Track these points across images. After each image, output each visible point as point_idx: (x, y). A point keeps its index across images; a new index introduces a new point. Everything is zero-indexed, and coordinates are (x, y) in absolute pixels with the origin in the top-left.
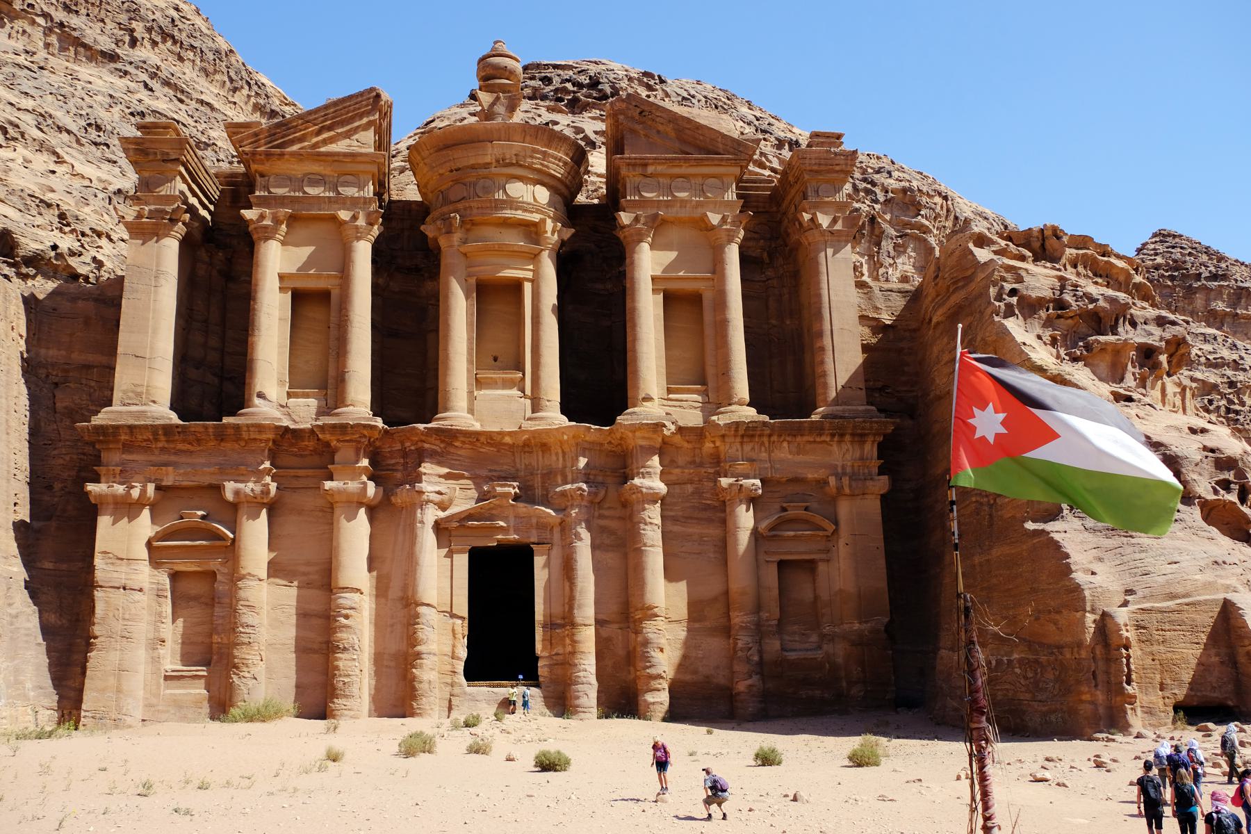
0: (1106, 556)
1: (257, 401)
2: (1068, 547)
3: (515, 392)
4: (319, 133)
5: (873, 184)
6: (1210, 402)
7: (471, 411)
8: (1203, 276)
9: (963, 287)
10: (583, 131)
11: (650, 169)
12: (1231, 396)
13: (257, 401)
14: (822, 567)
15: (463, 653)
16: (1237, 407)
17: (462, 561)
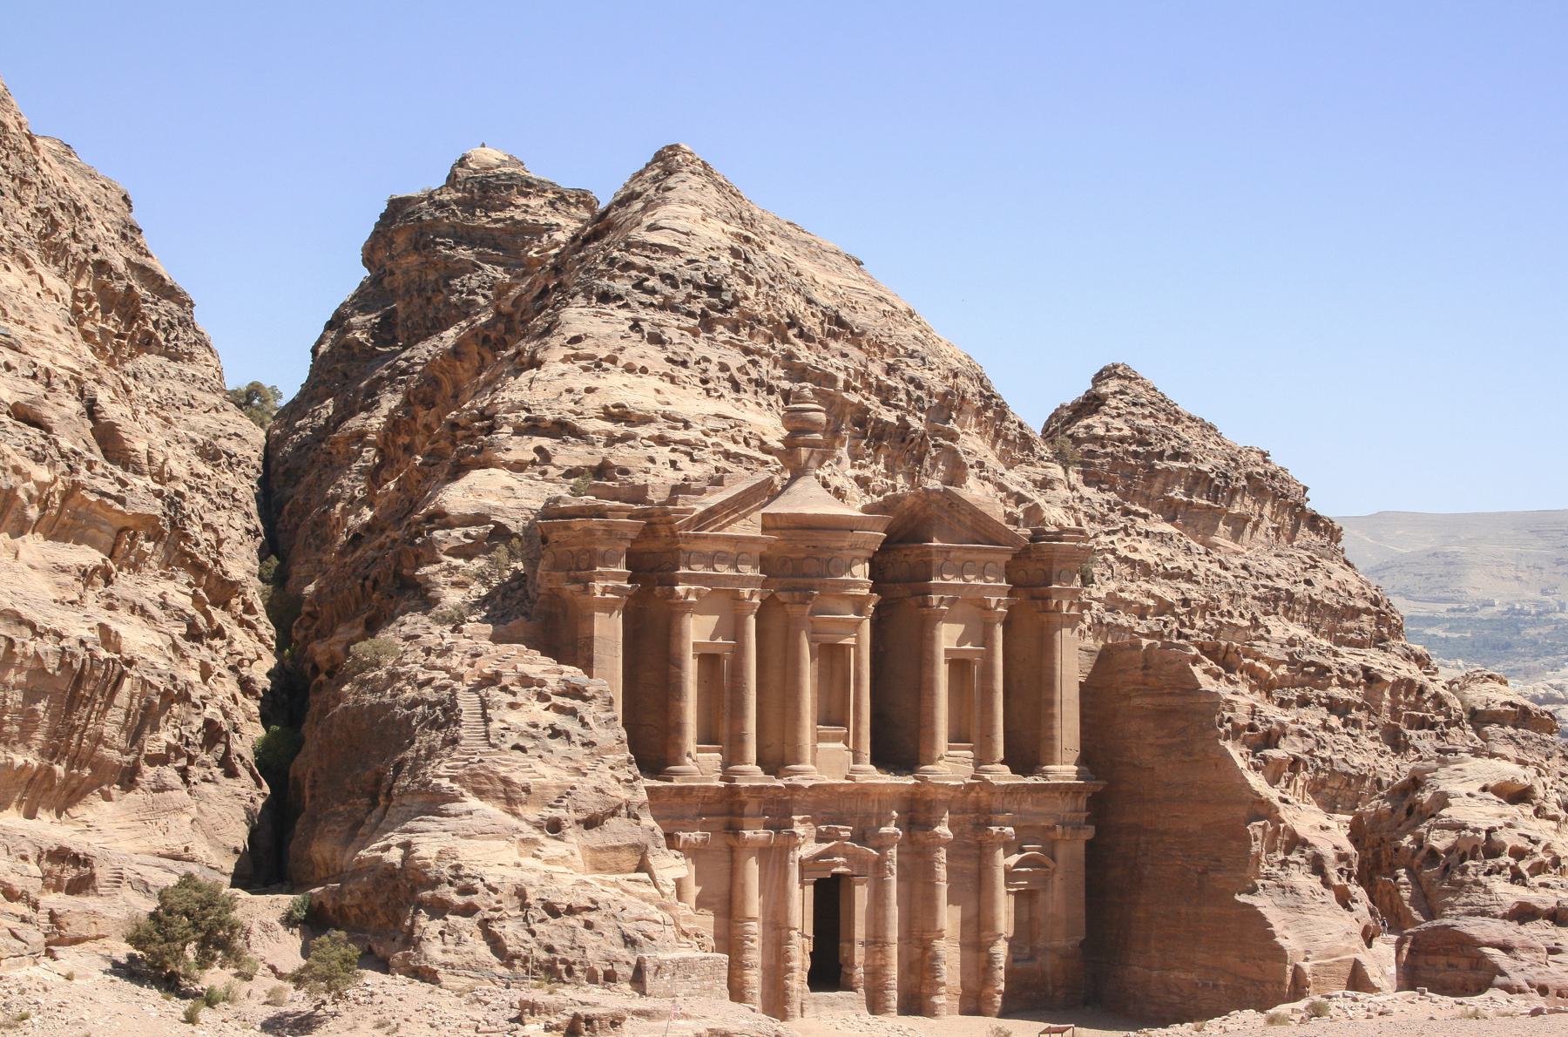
0: (1290, 925)
1: (688, 760)
2: (1271, 919)
3: (841, 745)
4: (727, 516)
5: (919, 386)
6: (1165, 624)
7: (814, 762)
8: (1167, 454)
9: (1179, 695)
10: (728, 370)
11: (952, 555)
12: (1183, 617)
13: (688, 760)
14: (1041, 896)
15: (808, 965)
16: (1186, 631)
17: (810, 889)
